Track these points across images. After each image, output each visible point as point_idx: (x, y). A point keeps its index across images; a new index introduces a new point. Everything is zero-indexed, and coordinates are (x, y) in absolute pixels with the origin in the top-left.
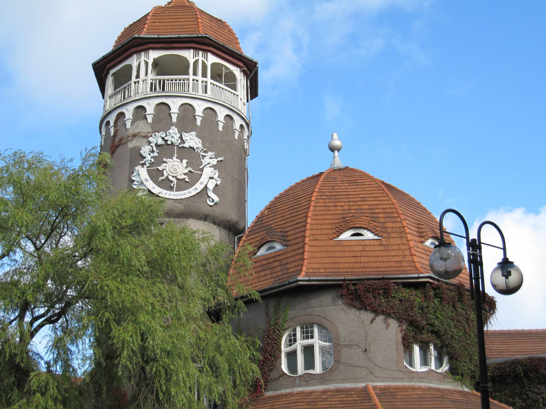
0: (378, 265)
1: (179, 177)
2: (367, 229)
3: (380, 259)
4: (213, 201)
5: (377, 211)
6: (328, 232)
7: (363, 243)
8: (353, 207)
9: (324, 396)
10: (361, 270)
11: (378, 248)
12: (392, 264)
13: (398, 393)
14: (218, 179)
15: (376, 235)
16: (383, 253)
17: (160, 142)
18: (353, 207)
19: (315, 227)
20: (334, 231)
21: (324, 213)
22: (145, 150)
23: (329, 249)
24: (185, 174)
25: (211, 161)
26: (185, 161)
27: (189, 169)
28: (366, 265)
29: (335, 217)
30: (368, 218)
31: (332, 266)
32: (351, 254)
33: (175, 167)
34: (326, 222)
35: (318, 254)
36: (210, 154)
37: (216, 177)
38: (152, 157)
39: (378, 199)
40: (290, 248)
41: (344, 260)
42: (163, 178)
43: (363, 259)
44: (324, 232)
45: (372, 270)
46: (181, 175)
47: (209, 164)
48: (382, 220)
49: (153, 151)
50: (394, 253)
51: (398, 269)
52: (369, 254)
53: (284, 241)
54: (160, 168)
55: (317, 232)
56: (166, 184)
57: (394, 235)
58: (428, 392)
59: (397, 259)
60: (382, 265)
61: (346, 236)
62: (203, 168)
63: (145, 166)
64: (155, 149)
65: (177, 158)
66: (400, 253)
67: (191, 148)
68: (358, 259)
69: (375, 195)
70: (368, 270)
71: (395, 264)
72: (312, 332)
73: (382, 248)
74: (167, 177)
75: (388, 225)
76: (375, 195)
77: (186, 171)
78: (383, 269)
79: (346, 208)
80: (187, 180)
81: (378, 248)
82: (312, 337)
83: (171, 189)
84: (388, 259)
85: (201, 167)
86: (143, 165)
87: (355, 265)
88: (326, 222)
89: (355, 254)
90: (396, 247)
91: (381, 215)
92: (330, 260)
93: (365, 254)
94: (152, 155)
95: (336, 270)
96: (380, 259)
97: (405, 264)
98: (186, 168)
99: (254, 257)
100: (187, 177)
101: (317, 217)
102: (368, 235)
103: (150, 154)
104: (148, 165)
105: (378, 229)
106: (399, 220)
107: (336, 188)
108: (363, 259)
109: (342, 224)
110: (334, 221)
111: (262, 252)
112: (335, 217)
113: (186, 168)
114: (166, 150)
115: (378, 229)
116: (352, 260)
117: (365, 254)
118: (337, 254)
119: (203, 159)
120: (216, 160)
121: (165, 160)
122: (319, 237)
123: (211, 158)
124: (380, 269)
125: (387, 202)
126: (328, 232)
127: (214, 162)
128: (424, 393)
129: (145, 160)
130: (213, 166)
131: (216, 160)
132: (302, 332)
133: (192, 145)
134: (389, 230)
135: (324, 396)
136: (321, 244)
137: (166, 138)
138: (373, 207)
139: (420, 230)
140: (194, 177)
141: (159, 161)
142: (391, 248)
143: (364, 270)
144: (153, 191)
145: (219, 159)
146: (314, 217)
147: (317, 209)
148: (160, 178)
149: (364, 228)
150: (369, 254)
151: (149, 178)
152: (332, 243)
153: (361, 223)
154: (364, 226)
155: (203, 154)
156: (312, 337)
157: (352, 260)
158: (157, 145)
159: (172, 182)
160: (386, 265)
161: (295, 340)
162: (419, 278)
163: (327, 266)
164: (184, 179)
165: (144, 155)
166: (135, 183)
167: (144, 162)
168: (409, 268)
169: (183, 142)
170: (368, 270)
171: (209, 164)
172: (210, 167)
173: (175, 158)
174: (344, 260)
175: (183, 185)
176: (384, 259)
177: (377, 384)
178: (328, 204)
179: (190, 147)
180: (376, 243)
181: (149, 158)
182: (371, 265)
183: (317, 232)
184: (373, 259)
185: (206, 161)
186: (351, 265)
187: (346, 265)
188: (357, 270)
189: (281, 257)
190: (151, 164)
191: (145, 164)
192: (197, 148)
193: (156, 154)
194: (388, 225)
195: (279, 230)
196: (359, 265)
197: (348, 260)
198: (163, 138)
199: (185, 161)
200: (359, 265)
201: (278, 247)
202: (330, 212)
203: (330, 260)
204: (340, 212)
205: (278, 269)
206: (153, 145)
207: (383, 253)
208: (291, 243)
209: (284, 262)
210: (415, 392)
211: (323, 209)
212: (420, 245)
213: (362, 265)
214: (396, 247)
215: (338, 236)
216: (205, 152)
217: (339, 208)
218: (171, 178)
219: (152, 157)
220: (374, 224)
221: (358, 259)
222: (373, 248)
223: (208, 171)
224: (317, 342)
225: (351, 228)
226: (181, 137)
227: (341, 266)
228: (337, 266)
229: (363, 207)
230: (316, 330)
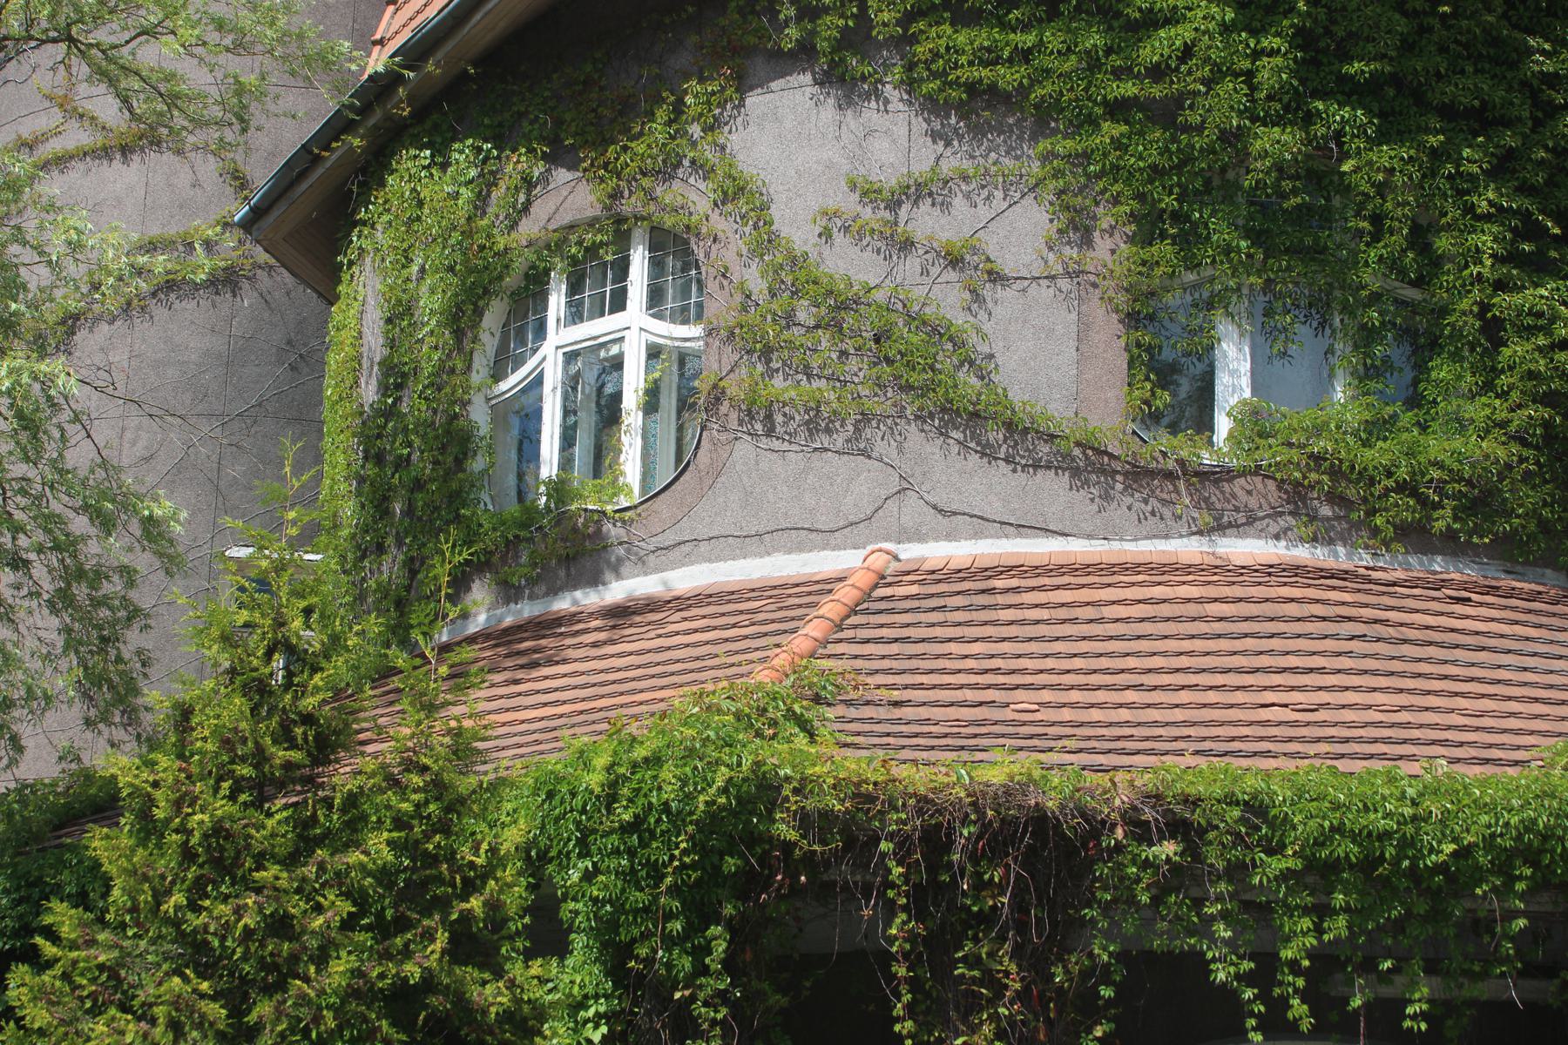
72: (622, 269)
82: (619, 303)
132: (575, 287)
161: (541, 331)
210: (1158, 592)
224: (635, 328)
230: (639, 261)
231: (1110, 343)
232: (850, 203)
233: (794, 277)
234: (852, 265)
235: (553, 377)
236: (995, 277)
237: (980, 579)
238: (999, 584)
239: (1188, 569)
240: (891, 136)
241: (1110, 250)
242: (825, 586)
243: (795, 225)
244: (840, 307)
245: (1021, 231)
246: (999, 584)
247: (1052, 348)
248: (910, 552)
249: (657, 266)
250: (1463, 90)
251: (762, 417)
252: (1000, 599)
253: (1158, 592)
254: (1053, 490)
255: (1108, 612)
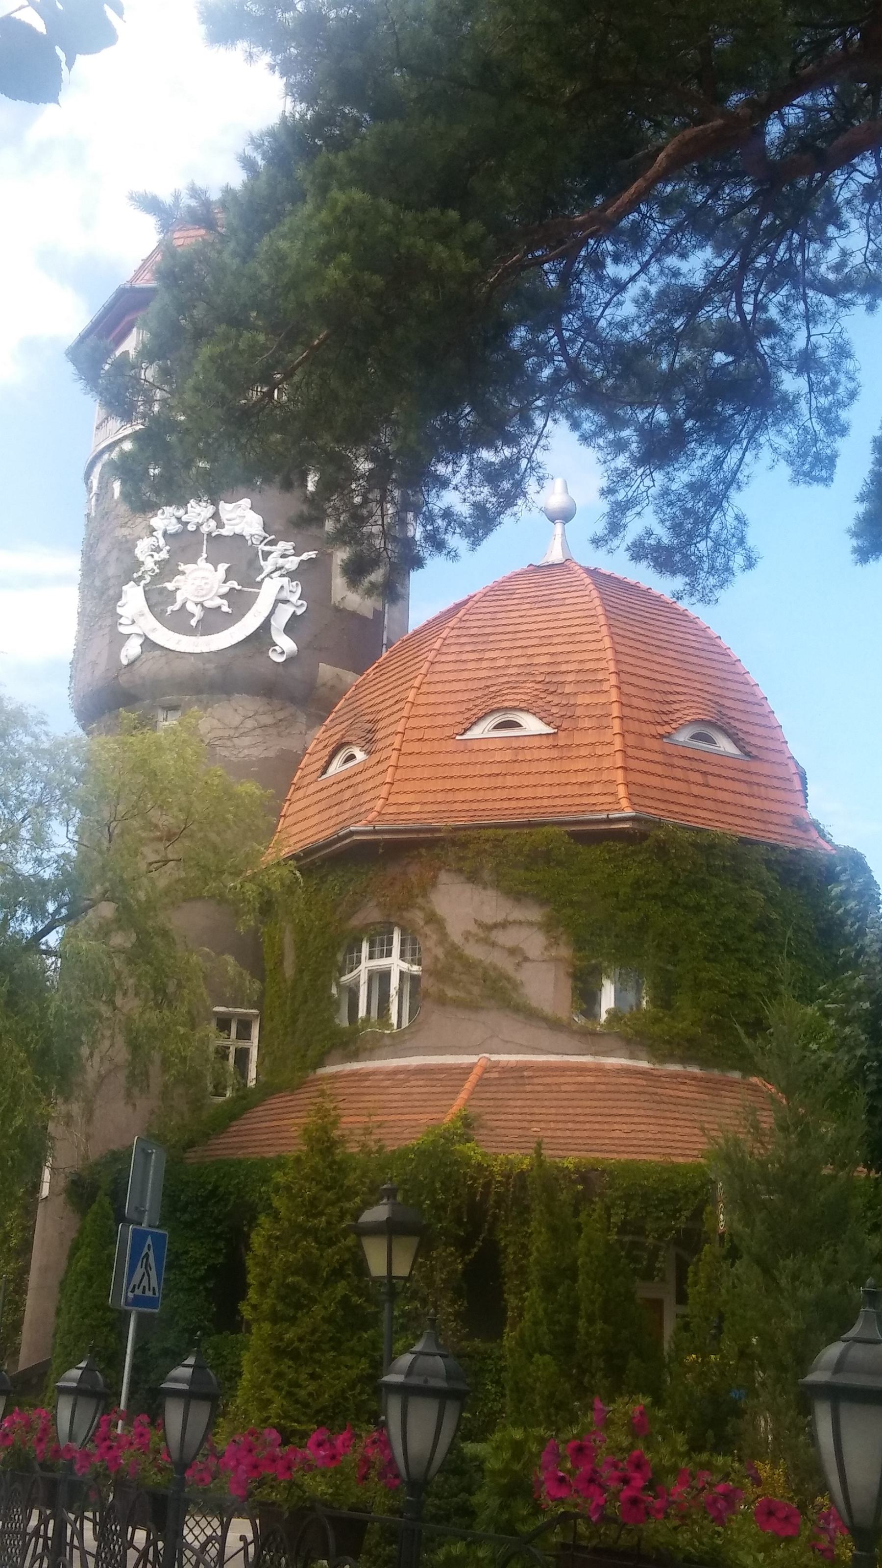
0: (540, 792)
1: (209, 604)
2: (528, 711)
3: (547, 779)
4: (283, 653)
5: (564, 668)
6: (449, 720)
7: (515, 745)
8: (514, 662)
9: (387, 1083)
10: (498, 805)
11: (545, 754)
12: (569, 790)
13: (536, 1081)
14: (300, 602)
15: (548, 724)
16: (556, 766)
17: (174, 527)
18: (514, 662)
19: (422, 711)
20: (459, 718)
21: (451, 676)
22: (142, 549)
23: (441, 759)
24: (222, 597)
25: (281, 561)
26: (223, 567)
27: (229, 584)
28: (513, 793)
29: (471, 685)
30: (537, 686)
31: (440, 797)
32: (487, 770)
33: (201, 583)
34: (447, 698)
35: (418, 773)
36: (282, 545)
37: (294, 598)
38: (156, 563)
39: (577, 638)
40: (376, 758)
41: (468, 783)
42: (176, 607)
43: (510, 781)
44: (440, 721)
45: (521, 804)
46: (211, 599)
47: (277, 569)
48: (568, 689)
49: (158, 549)
50: (580, 765)
51: (577, 801)
52: (525, 768)
53: (369, 742)
54: (170, 586)
55: (425, 722)
56: (179, 622)
57: (587, 723)
58: (613, 1080)
59: (581, 778)
60: (546, 792)
61: (482, 730)
62: (263, 579)
63: (142, 583)
64: (162, 542)
65: (207, 560)
66: (592, 764)
67: (239, 537)
68: (499, 782)
69: (573, 630)
70: (513, 804)
71: (576, 790)
72: (390, 942)
73: (555, 753)
74: (183, 605)
75: (580, 700)
76: (573, 630)
77: (225, 589)
78: (545, 802)
79: (500, 663)
80: (225, 609)
81: (545, 754)
82: (389, 954)
83: (191, 631)
84: (564, 779)
85: (258, 579)
86: (137, 581)
87: (489, 795)
88: (447, 698)
89: (495, 769)
90: (584, 752)
91: (570, 678)
92: (440, 785)
93: (517, 768)
94: (157, 557)
95: (443, 807)
96: (547, 779)
97: (596, 789)
98: (225, 582)
99: (324, 777)
100: (225, 602)
101: (432, 688)
102: (532, 725)
103: (152, 556)
104: (148, 579)
105: (554, 710)
106: (606, 686)
107: (499, 616)
108: (510, 781)
109: (478, 702)
110: (466, 696)
111: (336, 767)
112: (471, 685)
113: (225, 582)
114: (184, 545)
115: (554, 710)
116: (487, 782)
117: (517, 768)
118: (455, 771)
119: (265, 559)
120: (296, 560)
121: (182, 567)
122: (429, 734)
123: (283, 556)
124: (538, 803)
125: (592, 646)
126: (449, 720)
127: (292, 563)
128: (603, 1080)
129: (142, 569)
130: (292, 575)
131: (296, 560)
132: (372, 946)
133: (238, 531)
134: (579, 712)
135: (387, 1083)
136: (426, 748)
137: (185, 518)
138: (560, 659)
139: (666, 708)
140: (239, 602)
141: (168, 569)
142: (574, 753)
143: (506, 804)
144: (152, 637)
145: (305, 556)
146: (424, 688)
147: (438, 668)
148: (169, 609)
149: (521, 710)
150: (525, 768)
151: (146, 609)
152: (450, 745)
153: (519, 697)
154: (522, 705)
155: (267, 548)
156: (389, 954)
157: (487, 782)
158: (165, 534)
159: (193, 615)
160: (556, 791)
161: (359, 962)
162: (609, 821)
163: (430, 798)
164: (220, 607)
165: (141, 559)
166: (122, 621)
167: (140, 574)
168: (602, 799)
169: (220, 525)
170: (513, 804)
171: (277, 569)
172: (282, 576)
173: (201, 562)
174: (468, 783)
175: (214, 620)
176: (556, 779)
177: (504, 1058)
178: (464, 657)
179: (236, 535)
180: (546, 742)
181: (149, 564)
182: (523, 793)
183: (425, 722)
184: (532, 780)
185: (268, 566)
186: (481, 795)
187: (470, 796)
188: (489, 805)
189: (359, 778)
190: (158, 578)
191: (141, 578)
192: (252, 536)
193: (164, 555)
194: (580, 700)
195: (367, 718)
196: (499, 794)
197: (477, 783)
198: (179, 519)
199: (223, 567)
200: (499, 794)
201: (360, 756)
202: (466, 675)
203: (440, 785)
204: (484, 674)
205: (347, 806)
206: (159, 534)
207: (556, 766)
208: (380, 745)
209: (360, 788)
210: (580, 1079)
211: (450, 667)
212: (655, 744)
213: (505, 794)
214: (584, 752)
215: (466, 730)
216: (272, 543)
217: (485, 664)
218: (191, 607)
219: (156, 563)
220: (549, 698)
221: (499, 782)
222: (536, 754)
223: (270, 589)
224: (396, 964)
225: (493, 711)
226: (216, 516)
227: (460, 796)
228: (450, 797)
229: (536, 660)
231: (566, 985)
232: (473, 928)
233: (454, 952)
234: (474, 951)
235: (364, 978)
236: (526, 959)
237: (518, 1070)
238: (525, 1074)
239: (590, 1070)
240: (489, 905)
241: (564, 952)
242: (467, 1070)
243: (455, 934)
244: (469, 965)
245: (534, 942)
246: (525, 1074)
247: (544, 985)
248: (495, 1058)
249: (403, 943)
250: (693, 897)
251: (442, 1001)
252: (527, 1081)
253: (580, 1079)
254: (544, 1036)
255: (563, 1088)
